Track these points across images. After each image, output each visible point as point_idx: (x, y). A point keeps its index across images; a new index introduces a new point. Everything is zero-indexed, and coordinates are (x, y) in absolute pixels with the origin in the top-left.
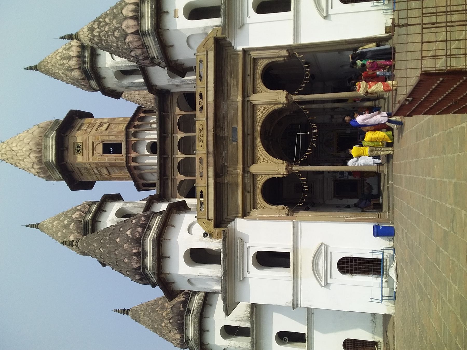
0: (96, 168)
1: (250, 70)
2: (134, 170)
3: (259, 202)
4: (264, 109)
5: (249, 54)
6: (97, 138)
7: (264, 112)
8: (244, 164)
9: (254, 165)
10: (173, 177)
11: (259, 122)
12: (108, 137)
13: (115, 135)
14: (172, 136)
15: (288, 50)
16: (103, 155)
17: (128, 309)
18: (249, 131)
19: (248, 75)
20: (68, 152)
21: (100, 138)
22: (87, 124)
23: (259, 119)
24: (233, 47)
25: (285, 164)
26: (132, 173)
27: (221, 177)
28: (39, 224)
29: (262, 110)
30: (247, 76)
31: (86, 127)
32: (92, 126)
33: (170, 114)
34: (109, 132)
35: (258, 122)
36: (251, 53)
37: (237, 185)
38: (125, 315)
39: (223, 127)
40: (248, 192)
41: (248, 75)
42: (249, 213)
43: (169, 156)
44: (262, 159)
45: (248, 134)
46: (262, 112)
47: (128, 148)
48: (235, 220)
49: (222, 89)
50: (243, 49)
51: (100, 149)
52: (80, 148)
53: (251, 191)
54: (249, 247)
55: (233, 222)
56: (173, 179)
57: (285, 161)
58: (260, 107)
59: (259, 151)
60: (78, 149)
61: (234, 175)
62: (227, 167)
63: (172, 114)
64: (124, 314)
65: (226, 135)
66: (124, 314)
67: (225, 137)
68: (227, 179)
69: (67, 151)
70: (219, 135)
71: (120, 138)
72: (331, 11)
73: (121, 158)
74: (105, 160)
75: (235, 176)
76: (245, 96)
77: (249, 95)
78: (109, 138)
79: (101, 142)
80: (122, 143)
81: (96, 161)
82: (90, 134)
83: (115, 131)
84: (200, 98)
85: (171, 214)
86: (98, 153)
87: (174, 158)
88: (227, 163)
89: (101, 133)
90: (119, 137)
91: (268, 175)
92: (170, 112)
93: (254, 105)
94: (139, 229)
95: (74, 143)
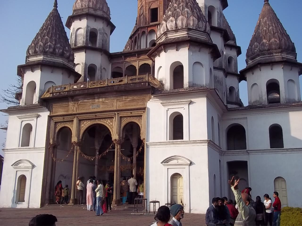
1: (135, 113)
2: (138, 33)
3: (59, 125)
5: (144, 112)
7: (110, 125)
10: (124, 63)
15: (144, 139)
18: (97, 116)
24: (149, 101)
25: (77, 141)
26: (137, 32)
29: (111, 123)
35: (104, 121)
37: (67, 111)
39: (100, 98)
43: (138, 58)
45: (96, 115)
48: (49, 111)
51: (154, 6)
53: (64, 120)
55: (47, 110)
57: (80, 141)
58: (113, 122)
65: (96, 101)
68: (71, 104)
78: (161, 11)
80: (158, 21)
84: (120, 81)
88: (80, 103)
94: (51, 50)
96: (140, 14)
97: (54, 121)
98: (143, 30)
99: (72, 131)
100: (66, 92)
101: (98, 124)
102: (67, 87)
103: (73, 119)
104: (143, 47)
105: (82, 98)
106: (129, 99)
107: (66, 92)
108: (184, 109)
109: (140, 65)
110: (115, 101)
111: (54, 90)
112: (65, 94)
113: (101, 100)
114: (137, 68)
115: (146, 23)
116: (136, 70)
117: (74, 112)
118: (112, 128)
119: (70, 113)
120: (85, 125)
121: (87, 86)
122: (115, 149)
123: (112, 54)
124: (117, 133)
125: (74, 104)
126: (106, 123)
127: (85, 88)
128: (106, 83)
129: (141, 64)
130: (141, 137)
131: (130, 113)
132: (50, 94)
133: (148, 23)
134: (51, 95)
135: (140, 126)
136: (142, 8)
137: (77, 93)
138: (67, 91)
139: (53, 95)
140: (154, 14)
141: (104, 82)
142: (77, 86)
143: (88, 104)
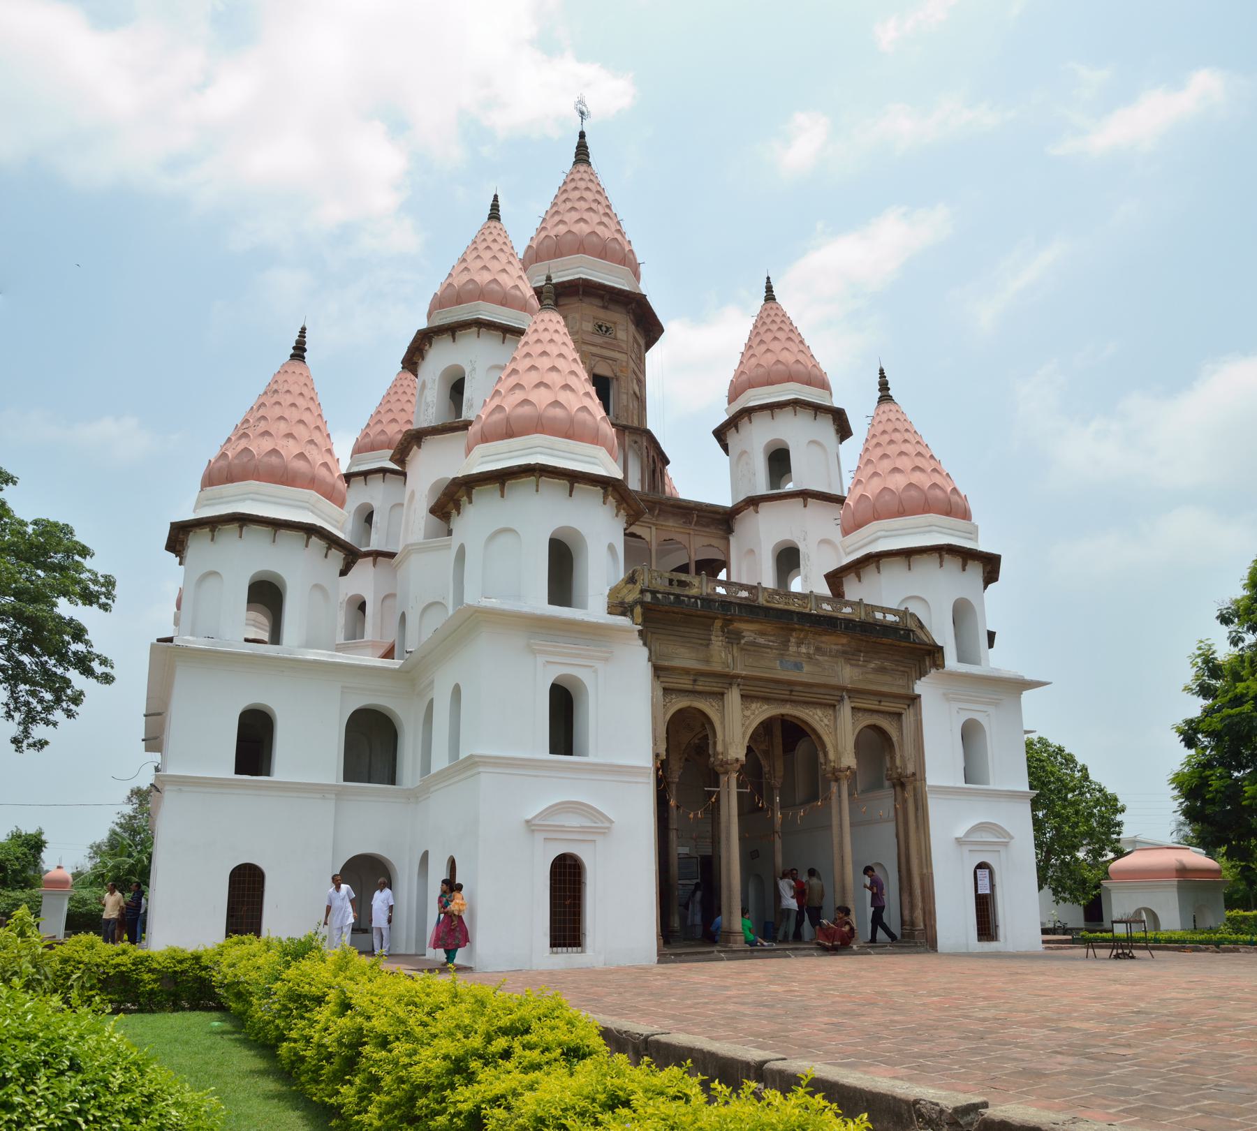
4: (826, 725)
5: (909, 706)
8: (744, 678)
14: (654, 524)
15: (914, 774)
17: (304, 358)
19: (880, 702)
20: (597, 306)
24: (920, 679)
27: (723, 631)
28: (499, 219)
29: (826, 721)
30: (879, 698)
33: (693, 527)
36: (912, 710)
37: (707, 661)
38: (292, 351)
40: (695, 681)
41: (880, 702)
42: (658, 677)
44: (748, 713)
45: (791, 691)
49: (861, 651)
50: (919, 696)
52: (606, 332)
54: (596, 671)
55: (641, 642)
60: (602, 329)
61: (723, 655)
63: (692, 532)
64: (294, 348)
66: (294, 348)
68: (717, 642)
69: (601, 305)
70: (791, 636)
72: (966, 849)
75: (721, 658)
76: (854, 693)
77: (852, 700)
88: (744, 644)
90: (625, 414)
91: (723, 723)
92: (696, 528)
95: (615, 323)
97: (663, 685)
102: (696, 585)
103: (726, 691)
105: (752, 631)
106: (872, 665)
108: (988, 715)
113: (803, 650)
119: (717, 668)
120: (762, 712)
121: (758, 597)
122: (738, 792)
125: (728, 642)
127: (753, 601)
128: (809, 606)
131: (877, 703)
134: (648, 598)
135: (895, 739)
141: (806, 601)
143: (768, 653)
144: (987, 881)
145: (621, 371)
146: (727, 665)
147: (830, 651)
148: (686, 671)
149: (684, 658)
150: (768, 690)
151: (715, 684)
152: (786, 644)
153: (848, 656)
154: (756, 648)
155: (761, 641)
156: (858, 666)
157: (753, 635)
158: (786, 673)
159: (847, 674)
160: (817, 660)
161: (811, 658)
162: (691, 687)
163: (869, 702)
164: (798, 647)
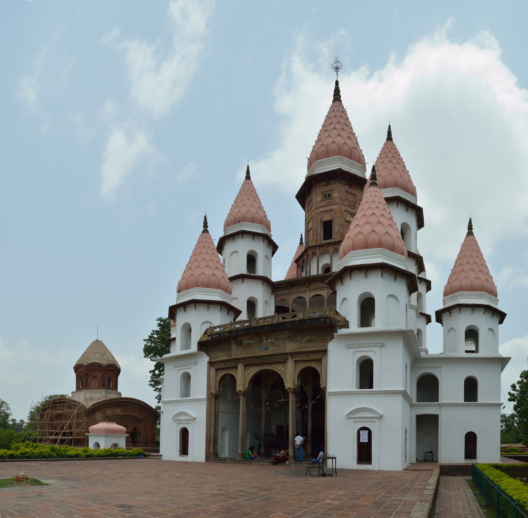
0: (312, 218)
2: (307, 255)
4: (283, 371)
6: (336, 213)
7: (282, 371)
8: (243, 358)
9: (244, 366)
10: (291, 294)
11: (274, 368)
12: (337, 224)
13: (338, 231)
16: (322, 223)
19: (308, 356)
21: (336, 216)
22: (354, 201)
23: (276, 367)
27: (235, 342)
29: (283, 369)
31: (351, 199)
32: (351, 206)
34: (342, 225)
35: (275, 366)
37: (230, 356)
40: (225, 364)
41: (308, 356)
43: (308, 287)
44: (249, 372)
45: (264, 360)
46: (281, 369)
47: (324, 246)
49: (298, 335)
51: (327, 218)
56: (289, 294)
59: (254, 369)
61: (236, 352)
62: (241, 346)
65: (263, 341)
67: (262, 341)
68: (234, 347)
71: (336, 236)
73: (319, 241)
74: (316, 225)
76: (292, 354)
78: (336, 225)
79: (333, 218)
81: (315, 216)
82: (341, 206)
83: (343, 229)
85: (220, 305)
86: (323, 218)
87: (307, 292)
88: (244, 345)
89: (342, 216)
93: (285, 362)
96: (308, 229)
98: (313, 250)
99: (236, 379)
100: (227, 334)
101: (267, 370)
102: (228, 327)
104: (314, 272)
105: (246, 339)
107: (227, 334)
109: (310, 297)
110: (288, 341)
111: (212, 332)
112: (226, 335)
113: (269, 341)
114: (308, 300)
115: (317, 241)
116: (306, 302)
117: (238, 356)
118: (285, 375)
119: (233, 357)
121: (252, 324)
123: (275, 283)
124: (291, 380)
125: (238, 346)
126: (278, 368)
129: (312, 296)
130: (320, 385)
131: (307, 357)
132: (207, 337)
133: (319, 241)
134: (210, 337)
136: (311, 220)
137: (241, 333)
138: (228, 332)
139: (212, 337)
140: (328, 226)
142: (240, 325)
143: (254, 346)
144: (366, 436)
145: (335, 214)
146: (237, 355)
147: (282, 338)
148: (222, 361)
149: (222, 356)
150: (254, 361)
151: (233, 364)
152: (261, 341)
153: (291, 339)
154: (249, 345)
155: (251, 342)
156: (296, 341)
157: (247, 340)
158: (262, 353)
159: (290, 347)
160: (276, 343)
161: (274, 344)
162: (225, 366)
163: (303, 357)
164: (267, 340)
